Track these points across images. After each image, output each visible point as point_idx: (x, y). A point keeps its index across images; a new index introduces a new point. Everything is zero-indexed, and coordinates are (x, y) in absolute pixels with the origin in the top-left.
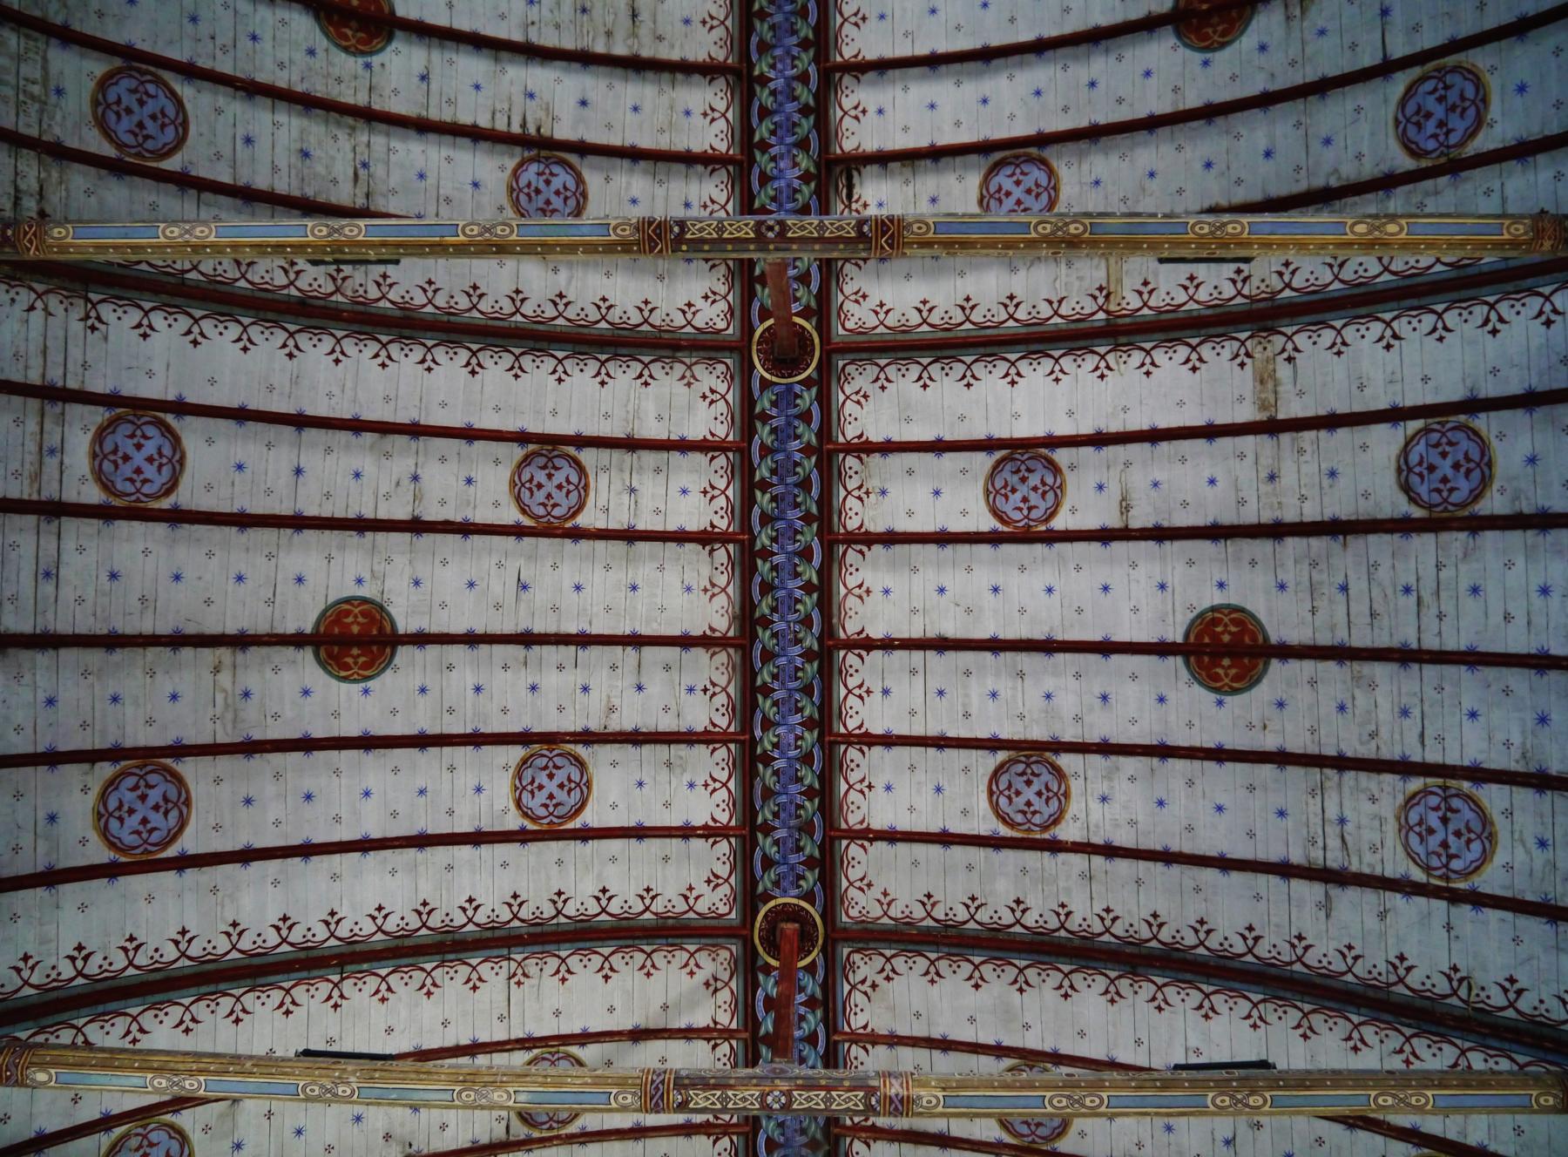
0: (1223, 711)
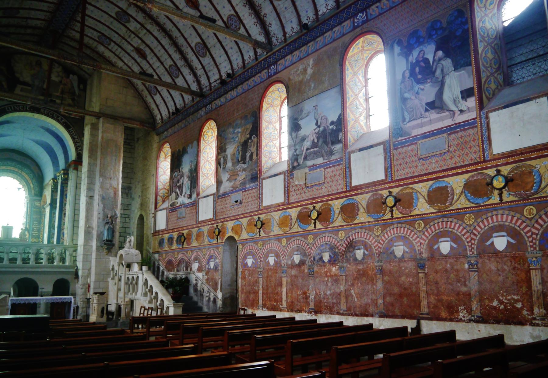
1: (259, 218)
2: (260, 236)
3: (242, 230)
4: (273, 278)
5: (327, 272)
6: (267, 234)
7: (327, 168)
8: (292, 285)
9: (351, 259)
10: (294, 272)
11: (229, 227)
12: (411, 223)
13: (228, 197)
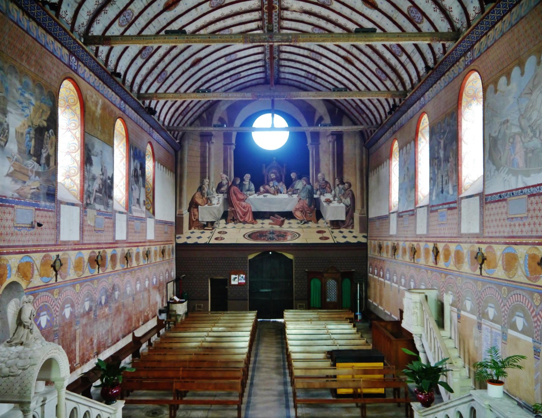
1: (58, 256)
2: (56, 281)
3: (33, 272)
4: (69, 334)
5: (103, 313)
6: (63, 279)
8: (83, 335)
10: (84, 321)
11: (12, 266)
12: (131, 272)
13: (10, 209)
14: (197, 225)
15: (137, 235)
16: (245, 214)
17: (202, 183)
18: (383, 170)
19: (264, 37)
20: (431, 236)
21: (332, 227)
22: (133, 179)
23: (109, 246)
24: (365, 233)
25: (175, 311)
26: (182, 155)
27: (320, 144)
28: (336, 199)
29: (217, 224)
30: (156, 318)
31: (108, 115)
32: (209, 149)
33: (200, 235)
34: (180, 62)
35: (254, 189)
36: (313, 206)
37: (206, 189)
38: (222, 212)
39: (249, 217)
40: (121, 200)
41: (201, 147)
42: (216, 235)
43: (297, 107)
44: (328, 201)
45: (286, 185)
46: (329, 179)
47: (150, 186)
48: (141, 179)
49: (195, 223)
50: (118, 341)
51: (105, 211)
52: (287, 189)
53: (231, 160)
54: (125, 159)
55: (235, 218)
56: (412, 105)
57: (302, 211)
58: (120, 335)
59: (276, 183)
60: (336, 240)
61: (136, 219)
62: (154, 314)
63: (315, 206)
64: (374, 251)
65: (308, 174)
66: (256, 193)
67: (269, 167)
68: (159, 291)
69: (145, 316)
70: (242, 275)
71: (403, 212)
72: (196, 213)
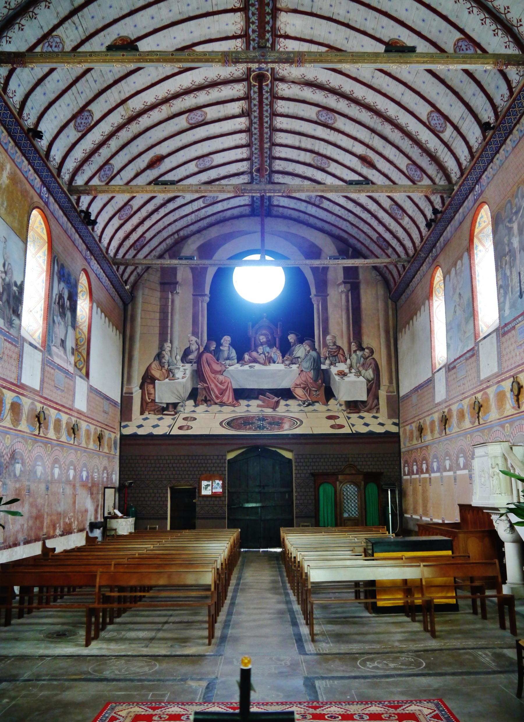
0: (117, 32)
7: (9, 342)
9: (12, 474)
12: (46, 444)
14: (153, 408)
15: (59, 392)
16: (222, 392)
17: (161, 348)
18: (419, 320)
19: (253, 55)
20: (506, 370)
21: (348, 411)
22: (56, 307)
23: (9, 386)
24: (396, 418)
25: (115, 530)
26: (134, 309)
27: (328, 295)
28: (353, 371)
29: (182, 406)
30: (84, 534)
31: (19, 194)
32: (173, 301)
33: (156, 422)
34: (133, 156)
35: (235, 357)
36: (320, 381)
37: (167, 357)
38: (189, 390)
39: (229, 397)
40: (35, 332)
41: (161, 299)
42: (180, 422)
43: (295, 246)
44: (342, 374)
45: (281, 352)
46: (343, 343)
47: (83, 336)
48: (69, 314)
49: (150, 405)
50: (15, 545)
51: (7, 330)
52: (283, 356)
53: (203, 316)
54: (45, 274)
55: (208, 398)
56: (461, 205)
57: (304, 388)
58: (21, 537)
59: (268, 349)
60: (355, 429)
61: (58, 369)
62: (81, 527)
63: (324, 381)
64: (411, 439)
65: (311, 336)
66: (238, 362)
67: (257, 326)
68: (92, 494)
69: (65, 524)
70: (217, 481)
71: (455, 360)
72: (152, 391)
